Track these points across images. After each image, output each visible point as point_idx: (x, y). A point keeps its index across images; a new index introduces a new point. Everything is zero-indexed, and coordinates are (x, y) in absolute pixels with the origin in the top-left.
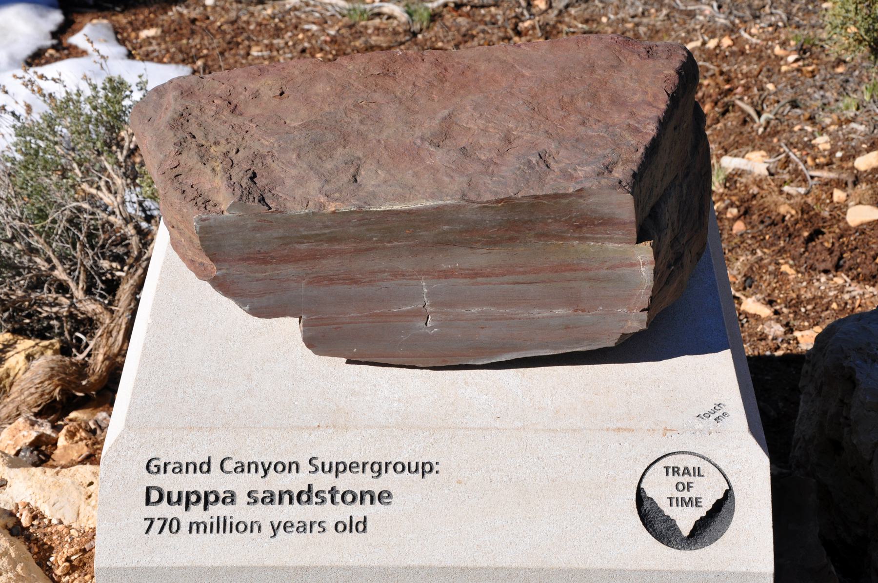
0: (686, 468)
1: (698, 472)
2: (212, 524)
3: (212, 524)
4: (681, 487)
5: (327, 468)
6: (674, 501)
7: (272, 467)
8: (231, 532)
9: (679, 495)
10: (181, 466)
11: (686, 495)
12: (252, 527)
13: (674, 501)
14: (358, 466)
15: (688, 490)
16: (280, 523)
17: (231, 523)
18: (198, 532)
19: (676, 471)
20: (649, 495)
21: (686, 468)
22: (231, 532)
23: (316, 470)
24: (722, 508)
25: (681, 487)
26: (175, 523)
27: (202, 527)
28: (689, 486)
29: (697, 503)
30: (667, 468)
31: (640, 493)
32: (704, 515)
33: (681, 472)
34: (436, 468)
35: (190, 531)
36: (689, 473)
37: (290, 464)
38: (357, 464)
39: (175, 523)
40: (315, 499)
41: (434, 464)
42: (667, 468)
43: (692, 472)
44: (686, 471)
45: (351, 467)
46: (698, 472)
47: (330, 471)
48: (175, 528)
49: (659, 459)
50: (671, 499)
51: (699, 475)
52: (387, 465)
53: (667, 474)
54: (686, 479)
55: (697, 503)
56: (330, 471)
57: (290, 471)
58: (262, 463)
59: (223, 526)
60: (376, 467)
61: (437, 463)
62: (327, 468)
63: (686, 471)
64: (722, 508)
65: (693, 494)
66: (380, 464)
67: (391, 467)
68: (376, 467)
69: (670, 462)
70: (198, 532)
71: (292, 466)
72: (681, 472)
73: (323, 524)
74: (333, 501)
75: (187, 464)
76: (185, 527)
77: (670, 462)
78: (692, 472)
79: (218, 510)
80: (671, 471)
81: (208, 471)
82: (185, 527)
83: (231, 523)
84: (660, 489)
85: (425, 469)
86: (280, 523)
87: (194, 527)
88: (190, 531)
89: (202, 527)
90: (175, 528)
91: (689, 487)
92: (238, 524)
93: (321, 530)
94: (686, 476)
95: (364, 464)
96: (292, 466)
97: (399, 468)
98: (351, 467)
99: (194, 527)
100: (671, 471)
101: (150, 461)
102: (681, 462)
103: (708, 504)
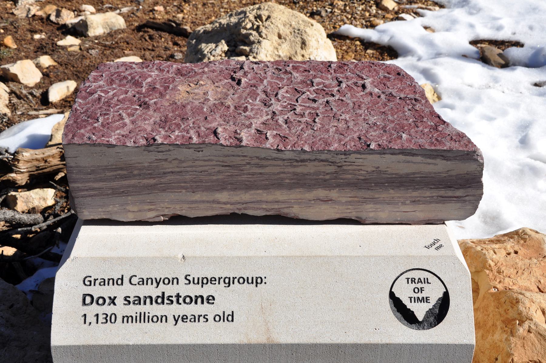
0: (419, 279)
1: (427, 281)
2: (136, 317)
3: (136, 317)
4: (416, 290)
5: (196, 281)
6: (413, 299)
7: (162, 281)
8: (148, 322)
9: (416, 295)
10: (104, 280)
11: (420, 295)
12: (163, 318)
13: (413, 299)
14: (215, 280)
15: (421, 292)
16: (179, 316)
17: (149, 316)
18: (128, 322)
19: (413, 280)
20: (397, 295)
21: (419, 279)
22: (148, 322)
23: (190, 283)
24: (444, 304)
25: (416, 290)
26: (113, 317)
27: (130, 319)
28: (422, 290)
29: (426, 300)
30: (408, 279)
31: (392, 295)
32: (431, 307)
33: (416, 281)
34: (264, 281)
35: (123, 322)
36: (421, 282)
37: (173, 279)
38: (215, 278)
39: (113, 317)
40: (166, 301)
41: (263, 278)
42: (408, 279)
43: (423, 282)
44: (420, 281)
45: (212, 280)
46: (427, 281)
47: (198, 283)
48: (113, 320)
49: (401, 274)
50: (411, 298)
51: (428, 283)
52: (234, 278)
53: (408, 283)
54: (419, 285)
55: (426, 300)
56: (198, 283)
57: (173, 284)
58: (156, 279)
59: (142, 318)
60: (227, 281)
61: (265, 278)
62: (196, 281)
63: (420, 281)
64: (444, 304)
65: (424, 295)
66: (229, 278)
67: (236, 280)
68: (227, 281)
69: (410, 275)
70: (128, 322)
71: (174, 281)
72: (416, 281)
73: (206, 317)
74: (178, 302)
75: (109, 279)
76: (119, 319)
77: (410, 275)
78: (423, 282)
79: (141, 308)
80: (410, 280)
81: (122, 284)
82: (119, 319)
83: (149, 316)
84: (404, 293)
85: (258, 281)
86: (179, 316)
87: (125, 319)
88: (123, 322)
89: (130, 319)
90: (113, 320)
91: (422, 290)
92: (153, 317)
93: (205, 320)
94: (420, 284)
95: (219, 279)
96: (174, 281)
97: (241, 281)
98: (212, 280)
99: (125, 319)
100: (410, 280)
101: (86, 277)
102: (416, 275)
103: (433, 301)
